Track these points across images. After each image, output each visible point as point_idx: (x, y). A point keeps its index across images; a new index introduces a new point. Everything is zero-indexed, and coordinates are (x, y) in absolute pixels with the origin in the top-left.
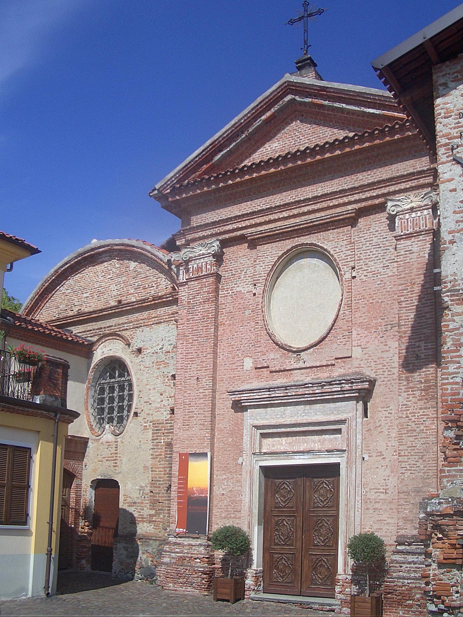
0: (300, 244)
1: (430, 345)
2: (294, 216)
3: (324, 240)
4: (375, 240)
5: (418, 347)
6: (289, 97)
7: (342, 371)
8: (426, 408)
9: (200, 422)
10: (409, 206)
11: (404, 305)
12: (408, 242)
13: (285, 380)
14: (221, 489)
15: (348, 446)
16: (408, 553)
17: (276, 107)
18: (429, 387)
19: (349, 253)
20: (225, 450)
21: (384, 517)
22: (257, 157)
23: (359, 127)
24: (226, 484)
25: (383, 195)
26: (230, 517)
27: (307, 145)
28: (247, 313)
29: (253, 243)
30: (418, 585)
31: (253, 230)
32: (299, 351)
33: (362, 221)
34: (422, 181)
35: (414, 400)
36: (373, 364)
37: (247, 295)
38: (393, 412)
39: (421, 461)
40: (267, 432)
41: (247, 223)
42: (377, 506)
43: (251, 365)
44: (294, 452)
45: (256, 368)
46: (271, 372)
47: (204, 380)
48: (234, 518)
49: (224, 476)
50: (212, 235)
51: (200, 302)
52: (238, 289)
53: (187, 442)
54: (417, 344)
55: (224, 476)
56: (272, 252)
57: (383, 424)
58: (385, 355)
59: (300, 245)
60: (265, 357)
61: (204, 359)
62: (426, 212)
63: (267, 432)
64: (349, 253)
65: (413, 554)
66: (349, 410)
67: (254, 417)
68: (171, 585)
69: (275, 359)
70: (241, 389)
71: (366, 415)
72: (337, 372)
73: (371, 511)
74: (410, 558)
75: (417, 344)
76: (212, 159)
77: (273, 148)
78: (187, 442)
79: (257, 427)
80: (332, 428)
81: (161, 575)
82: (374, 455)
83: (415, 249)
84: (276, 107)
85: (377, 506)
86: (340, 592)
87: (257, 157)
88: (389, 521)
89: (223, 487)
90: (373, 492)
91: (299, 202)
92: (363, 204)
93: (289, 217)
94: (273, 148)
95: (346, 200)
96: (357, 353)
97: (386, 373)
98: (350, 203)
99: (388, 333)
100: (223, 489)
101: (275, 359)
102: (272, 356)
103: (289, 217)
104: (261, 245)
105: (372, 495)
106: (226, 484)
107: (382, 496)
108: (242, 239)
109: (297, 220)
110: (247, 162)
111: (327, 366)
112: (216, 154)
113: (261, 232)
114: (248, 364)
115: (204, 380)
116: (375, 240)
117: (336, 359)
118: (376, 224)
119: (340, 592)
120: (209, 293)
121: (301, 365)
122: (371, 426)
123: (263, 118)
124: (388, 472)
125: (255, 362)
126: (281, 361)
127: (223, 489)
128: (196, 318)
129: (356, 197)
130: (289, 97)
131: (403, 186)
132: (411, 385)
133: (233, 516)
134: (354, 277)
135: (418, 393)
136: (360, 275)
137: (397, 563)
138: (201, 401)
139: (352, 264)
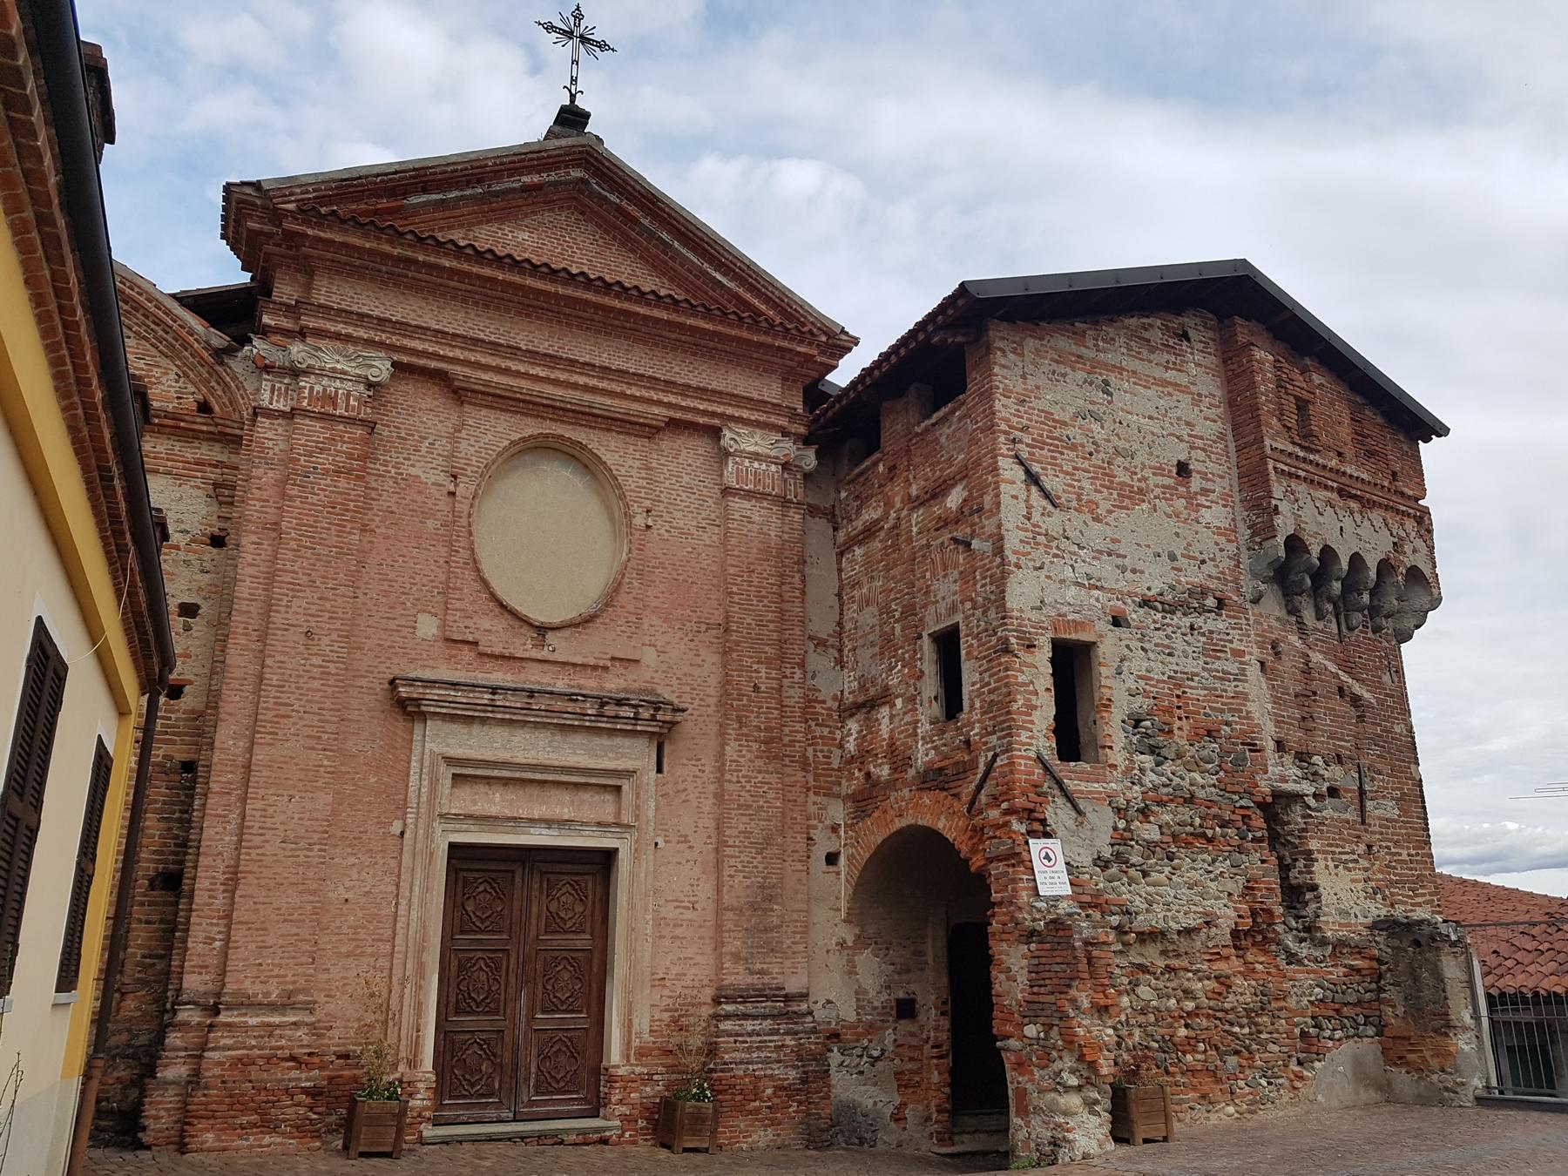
0: (560, 432)
1: (773, 673)
2: (556, 382)
3: (610, 449)
4: (686, 479)
5: (757, 671)
6: (576, 173)
7: (621, 683)
8: (767, 772)
9: (309, 731)
10: (752, 449)
11: (736, 598)
12: (747, 505)
13: (509, 677)
14: (341, 888)
15: (637, 818)
16: (745, 1016)
17: (553, 177)
18: (773, 738)
19: (643, 483)
20: (359, 802)
21: (690, 953)
22: (486, 236)
23: (679, 286)
24: (355, 876)
25: (721, 416)
26: (363, 954)
27: (585, 269)
28: (430, 524)
29: (459, 394)
30: (769, 1072)
31: (467, 371)
32: (542, 630)
33: (667, 443)
34: (773, 419)
35: (749, 756)
36: (675, 682)
37: (433, 490)
38: (707, 769)
39: (759, 858)
40: (466, 774)
41: (458, 353)
42: (678, 931)
43: (435, 631)
44: (531, 820)
45: (447, 640)
46: (482, 655)
47: (326, 640)
48: (372, 955)
49: (352, 860)
50: (381, 345)
51: (328, 471)
52: (413, 471)
53: (265, 773)
54: (755, 667)
55: (352, 860)
56: (499, 430)
57: (690, 788)
58: (696, 671)
59: (554, 436)
60: (468, 623)
61: (330, 594)
62: (773, 468)
63: (466, 774)
64: (643, 483)
65: (755, 1017)
66: (634, 755)
67: (440, 741)
68: (210, 1136)
69: (493, 632)
70: (428, 675)
71: (659, 770)
72: (613, 684)
73: (667, 942)
74: (749, 1025)
75: (755, 667)
76: (405, 195)
77: (518, 239)
78: (265, 773)
79: (450, 761)
80: (611, 785)
81: (163, 1113)
82: (674, 839)
83: (756, 518)
84: (553, 177)
85: (678, 931)
86: (621, 1102)
87: (486, 236)
88: (698, 959)
89: (348, 884)
90: (671, 905)
91: (572, 362)
92: (679, 415)
93: (547, 380)
94: (518, 239)
95: (654, 395)
96: (649, 656)
97: (697, 702)
98: (659, 403)
99: (701, 637)
100: (347, 889)
101: (493, 632)
102: (486, 624)
103: (547, 380)
104: (475, 404)
105: (669, 912)
106: (355, 876)
107: (688, 914)
108: (440, 378)
109: (559, 392)
110: (458, 236)
111: (595, 668)
112: (415, 192)
113: (487, 384)
114: (428, 627)
115: (326, 640)
116: (686, 479)
117: (613, 659)
118: (688, 454)
119: (621, 1102)
120: (350, 456)
121: (544, 654)
122: (670, 789)
123: (526, 179)
124: (697, 872)
125: (444, 625)
126: (505, 638)
127: (347, 889)
128: (312, 499)
129: (671, 399)
130: (576, 173)
131: (745, 414)
132: (745, 730)
133: (370, 950)
134: (648, 527)
135: (755, 746)
136: (660, 528)
137: (730, 1035)
138: (316, 684)
139: (648, 503)
